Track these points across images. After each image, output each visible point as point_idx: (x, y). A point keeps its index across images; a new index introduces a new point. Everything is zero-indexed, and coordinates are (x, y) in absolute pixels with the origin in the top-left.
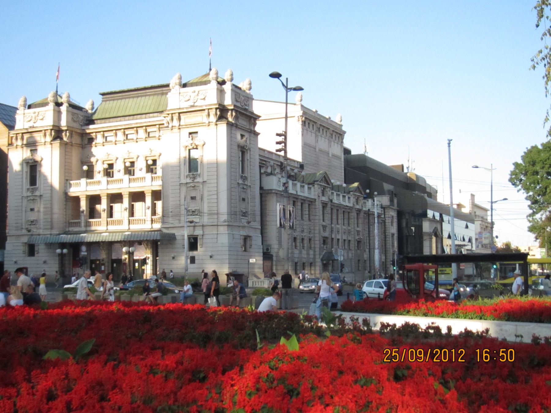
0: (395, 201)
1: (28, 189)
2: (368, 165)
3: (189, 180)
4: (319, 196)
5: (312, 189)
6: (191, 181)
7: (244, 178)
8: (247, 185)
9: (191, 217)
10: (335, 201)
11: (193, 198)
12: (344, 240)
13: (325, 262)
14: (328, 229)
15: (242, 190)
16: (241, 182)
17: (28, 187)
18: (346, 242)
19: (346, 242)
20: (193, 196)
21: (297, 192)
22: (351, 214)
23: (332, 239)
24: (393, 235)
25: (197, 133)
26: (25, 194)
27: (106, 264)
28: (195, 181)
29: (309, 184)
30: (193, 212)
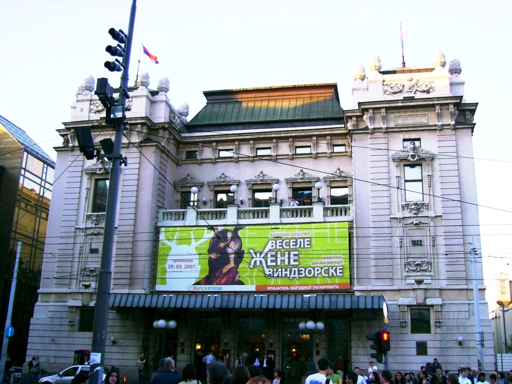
1: (89, 217)
3: (407, 214)
9: (414, 274)
11: (416, 243)
20: (416, 239)
25: (419, 140)
26: (83, 226)
27: (232, 352)
28: (419, 215)
30: (418, 265)
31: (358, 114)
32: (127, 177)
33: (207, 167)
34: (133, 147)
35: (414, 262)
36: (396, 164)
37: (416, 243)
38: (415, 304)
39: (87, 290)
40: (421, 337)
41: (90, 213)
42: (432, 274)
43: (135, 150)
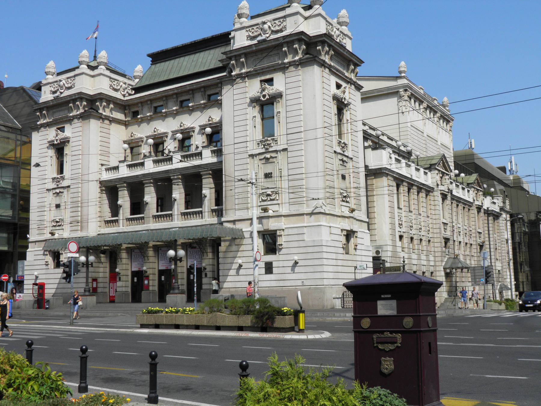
0: (507, 202)
1: (53, 179)
2: (476, 161)
4: (438, 185)
5: (429, 173)
6: (263, 150)
7: (344, 146)
8: (347, 157)
10: (454, 193)
11: (268, 176)
12: (466, 243)
13: (448, 271)
14: (449, 228)
15: (341, 162)
16: (339, 150)
17: (55, 175)
18: (468, 245)
19: (468, 245)
21: (411, 176)
22: (471, 211)
23: (454, 241)
24: (507, 240)
28: (271, 149)
29: (425, 169)
30: (268, 195)
32: (74, 144)
33: (144, 125)
39: (53, 237)
40: (270, 258)
41: (55, 175)
42: (279, 202)
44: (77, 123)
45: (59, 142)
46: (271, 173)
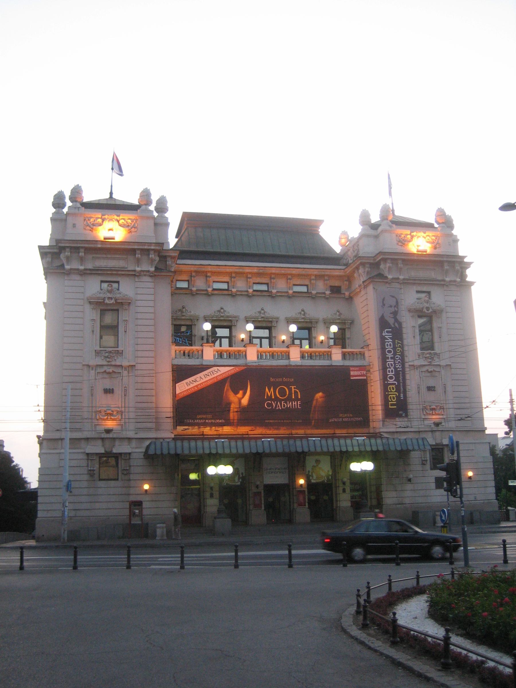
1: (97, 353)
3: (422, 362)
11: (430, 389)
31: (372, 261)
34: (145, 275)
35: (430, 406)
36: (411, 314)
37: (430, 389)
38: (434, 444)
43: (148, 279)
44: (147, 283)
45: (113, 301)
46: (434, 387)
